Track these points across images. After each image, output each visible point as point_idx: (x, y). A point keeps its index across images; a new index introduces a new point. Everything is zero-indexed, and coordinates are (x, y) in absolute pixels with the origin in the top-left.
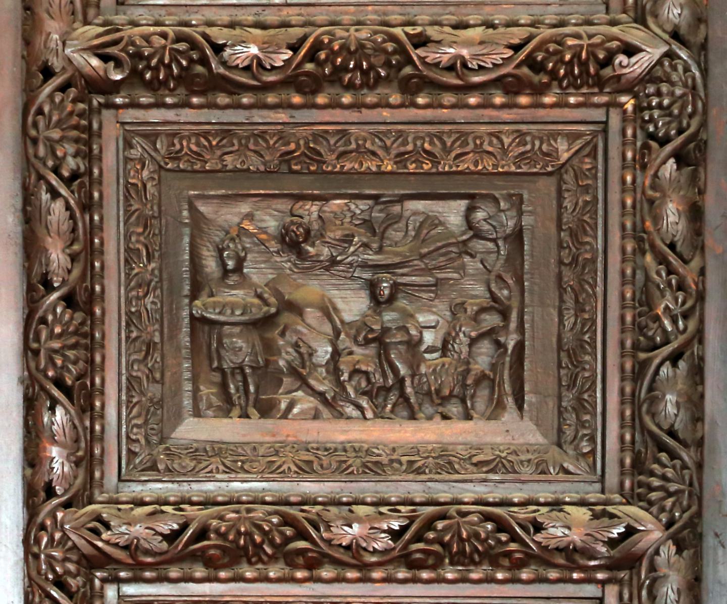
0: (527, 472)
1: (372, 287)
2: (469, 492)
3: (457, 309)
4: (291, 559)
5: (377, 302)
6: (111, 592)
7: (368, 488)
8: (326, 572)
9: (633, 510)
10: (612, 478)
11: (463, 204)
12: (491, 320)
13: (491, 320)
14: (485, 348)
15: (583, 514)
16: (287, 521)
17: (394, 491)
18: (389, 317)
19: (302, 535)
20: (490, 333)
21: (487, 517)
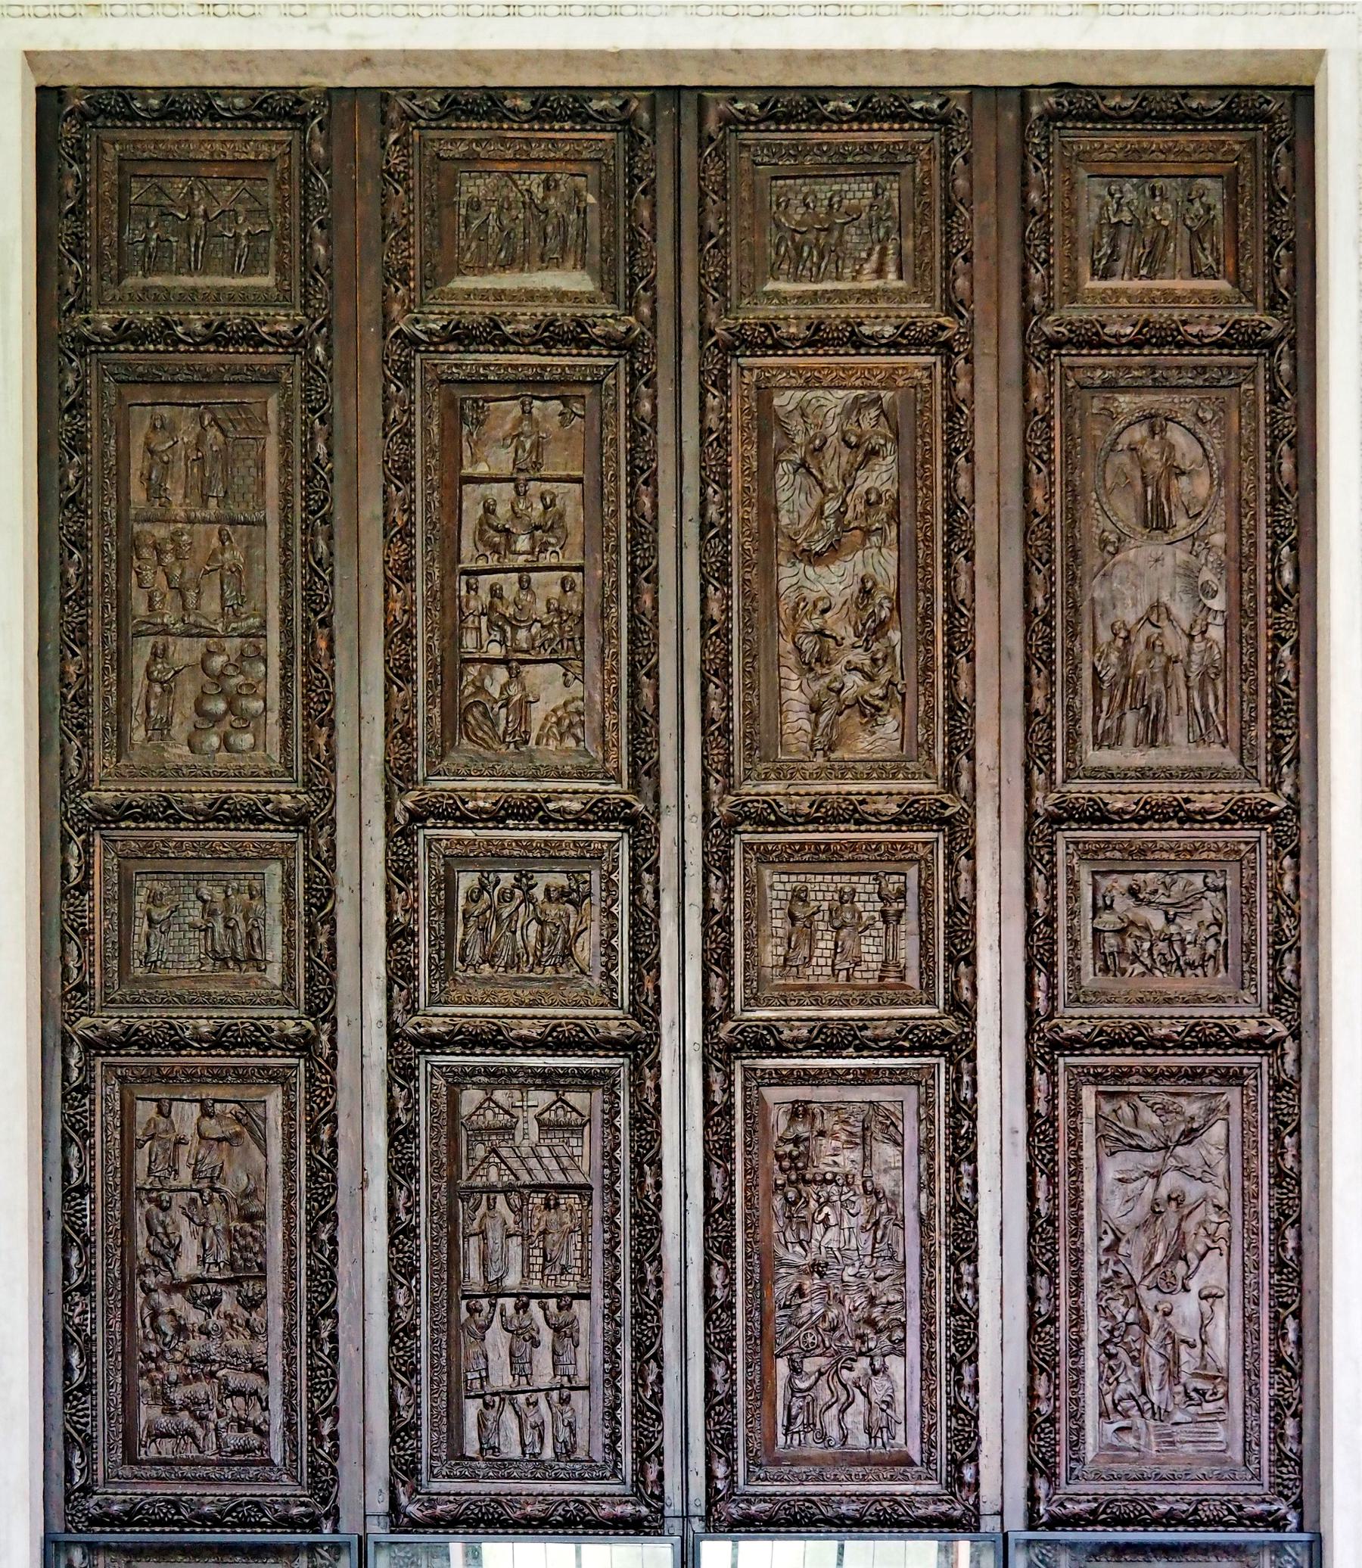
0: (1232, 1003)
1: (1166, 913)
2: (1207, 1013)
3: (1200, 923)
4: (1136, 1045)
5: (1169, 921)
6: (1061, 1061)
7: (1166, 1011)
8: (1150, 1051)
9: (1274, 1020)
10: (1265, 1006)
11: (1201, 876)
12: (1214, 929)
13: (1214, 929)
14: (1212, 941)
15: (1254, 1022)
16: (1135, 1027)
17: (1177, 1012)
18: (1173, 929)
19: (1141, 1034)
20: (1215, 935)
21: (1216, 1025)
